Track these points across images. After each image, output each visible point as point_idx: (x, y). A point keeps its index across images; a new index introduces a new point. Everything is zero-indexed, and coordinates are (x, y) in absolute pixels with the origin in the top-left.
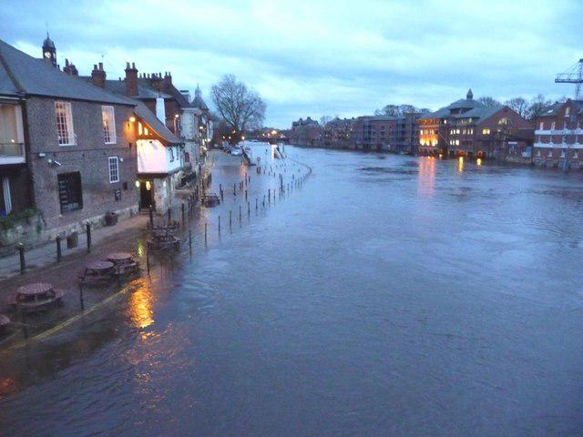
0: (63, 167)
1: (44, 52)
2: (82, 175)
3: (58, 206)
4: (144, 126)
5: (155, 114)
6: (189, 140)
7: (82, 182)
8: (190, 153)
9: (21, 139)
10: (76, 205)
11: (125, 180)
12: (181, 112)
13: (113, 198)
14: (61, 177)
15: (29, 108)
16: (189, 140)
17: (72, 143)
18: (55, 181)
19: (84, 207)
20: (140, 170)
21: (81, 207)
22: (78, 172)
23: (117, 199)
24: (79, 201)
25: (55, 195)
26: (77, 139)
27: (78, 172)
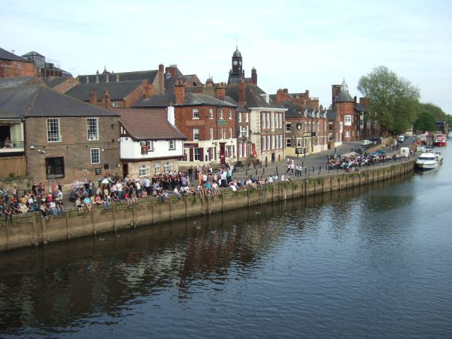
0: (50, 155)
1: (233, 61)
2: (65, 158)
3: (45, 175)
4: (124, 129)
5: (167, 118)
6: (255, 134)
7: (65, 162)
8: (256, 144)
9: (23, 140)
10: (61, 175)
11: (106, 162)
12: (250, 111)
13: (94, 173)
14: (47, 159)
15: (27, 123)
16: (255, 134)
17: (60, 141)
18: (43, 162)
19: (66, 175)
20: (123, 156)
21: (64, 177)
22: (62, 159)
23: (97, 174)
24: (63, 172)
25: (43, 169)
26: (63, 138)
27: (62, 159)
